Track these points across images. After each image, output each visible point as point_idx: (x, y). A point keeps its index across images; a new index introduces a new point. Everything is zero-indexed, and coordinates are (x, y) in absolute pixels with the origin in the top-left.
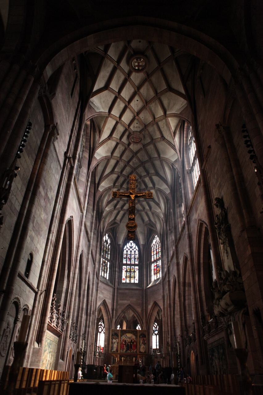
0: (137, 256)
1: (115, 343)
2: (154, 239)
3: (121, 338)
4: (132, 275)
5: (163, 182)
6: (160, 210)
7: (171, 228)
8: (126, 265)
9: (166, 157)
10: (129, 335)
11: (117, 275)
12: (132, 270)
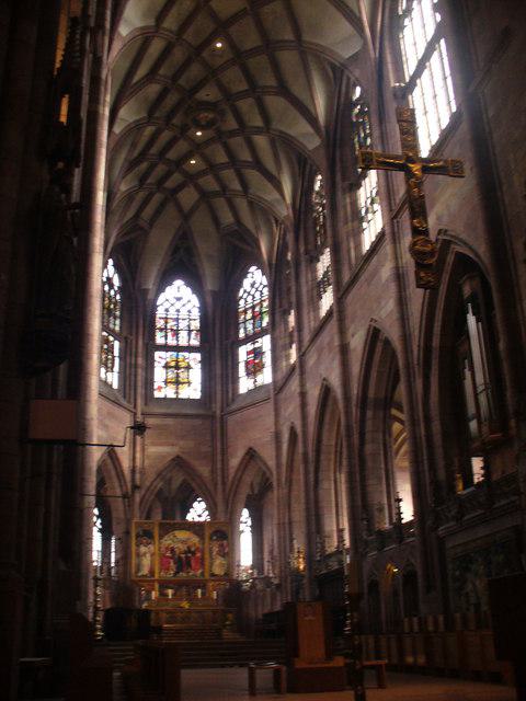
0: (196, 324)
1: (145, 554)
2: (246, 277)
3: (160, 543)
4: (183, 376)
5: (298, 114)
6: (277, 195)
7: (310, 247)
8: (166, 348)
9: (322, 43)
10: (182, 535)
11: (139, 378)
12: (183, 364)
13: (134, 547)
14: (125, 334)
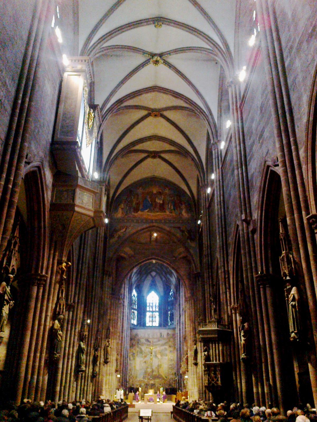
0: (157, 304)
4: (154, 319)
12: (154, 316)
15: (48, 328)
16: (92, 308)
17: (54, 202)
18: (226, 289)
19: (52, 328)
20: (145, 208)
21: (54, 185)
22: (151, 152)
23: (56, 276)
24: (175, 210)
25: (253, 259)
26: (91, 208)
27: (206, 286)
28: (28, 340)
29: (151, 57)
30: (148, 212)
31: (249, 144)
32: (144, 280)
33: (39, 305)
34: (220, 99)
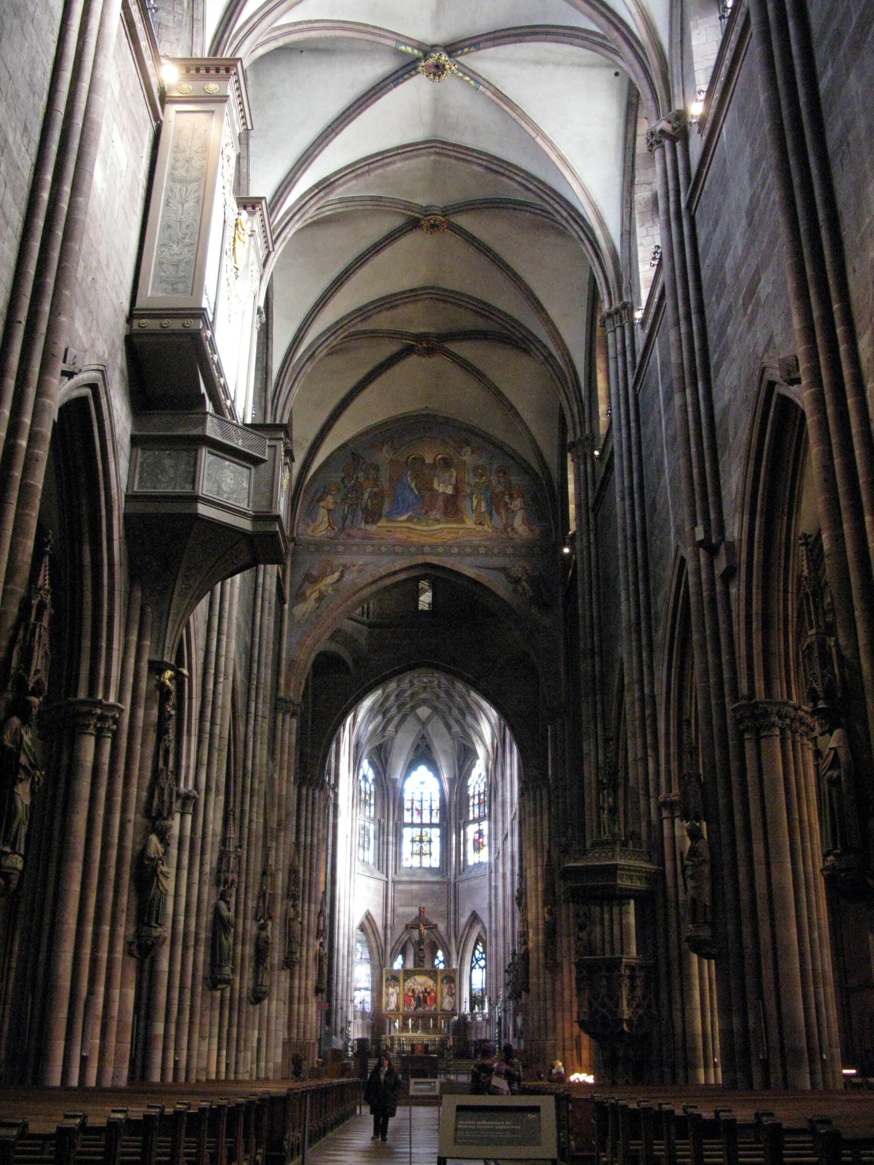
0: (436, 805)
4: (426, 848)
10: (421, 979)
11: (390, 853)
12: (425, 839)
13: (384, 988)
14: (378, 817)
15: (129, 855)
16: (247, 807)
17: (135, 489)
18: (645, 747)
19: (141, 856)
20: (398, 508)
21: (135, 441)
22: (420, 337)
23: (146, 709)
24: (491, 514)
25: (725, 658)
26: (243, 505)
27: (585, 745)
28: (76, 887)
29: (421, 54)
30: (410, 519)
31: (717, 317)
32: (396, 732)
33: (102, 792)
34: (628, 179)
